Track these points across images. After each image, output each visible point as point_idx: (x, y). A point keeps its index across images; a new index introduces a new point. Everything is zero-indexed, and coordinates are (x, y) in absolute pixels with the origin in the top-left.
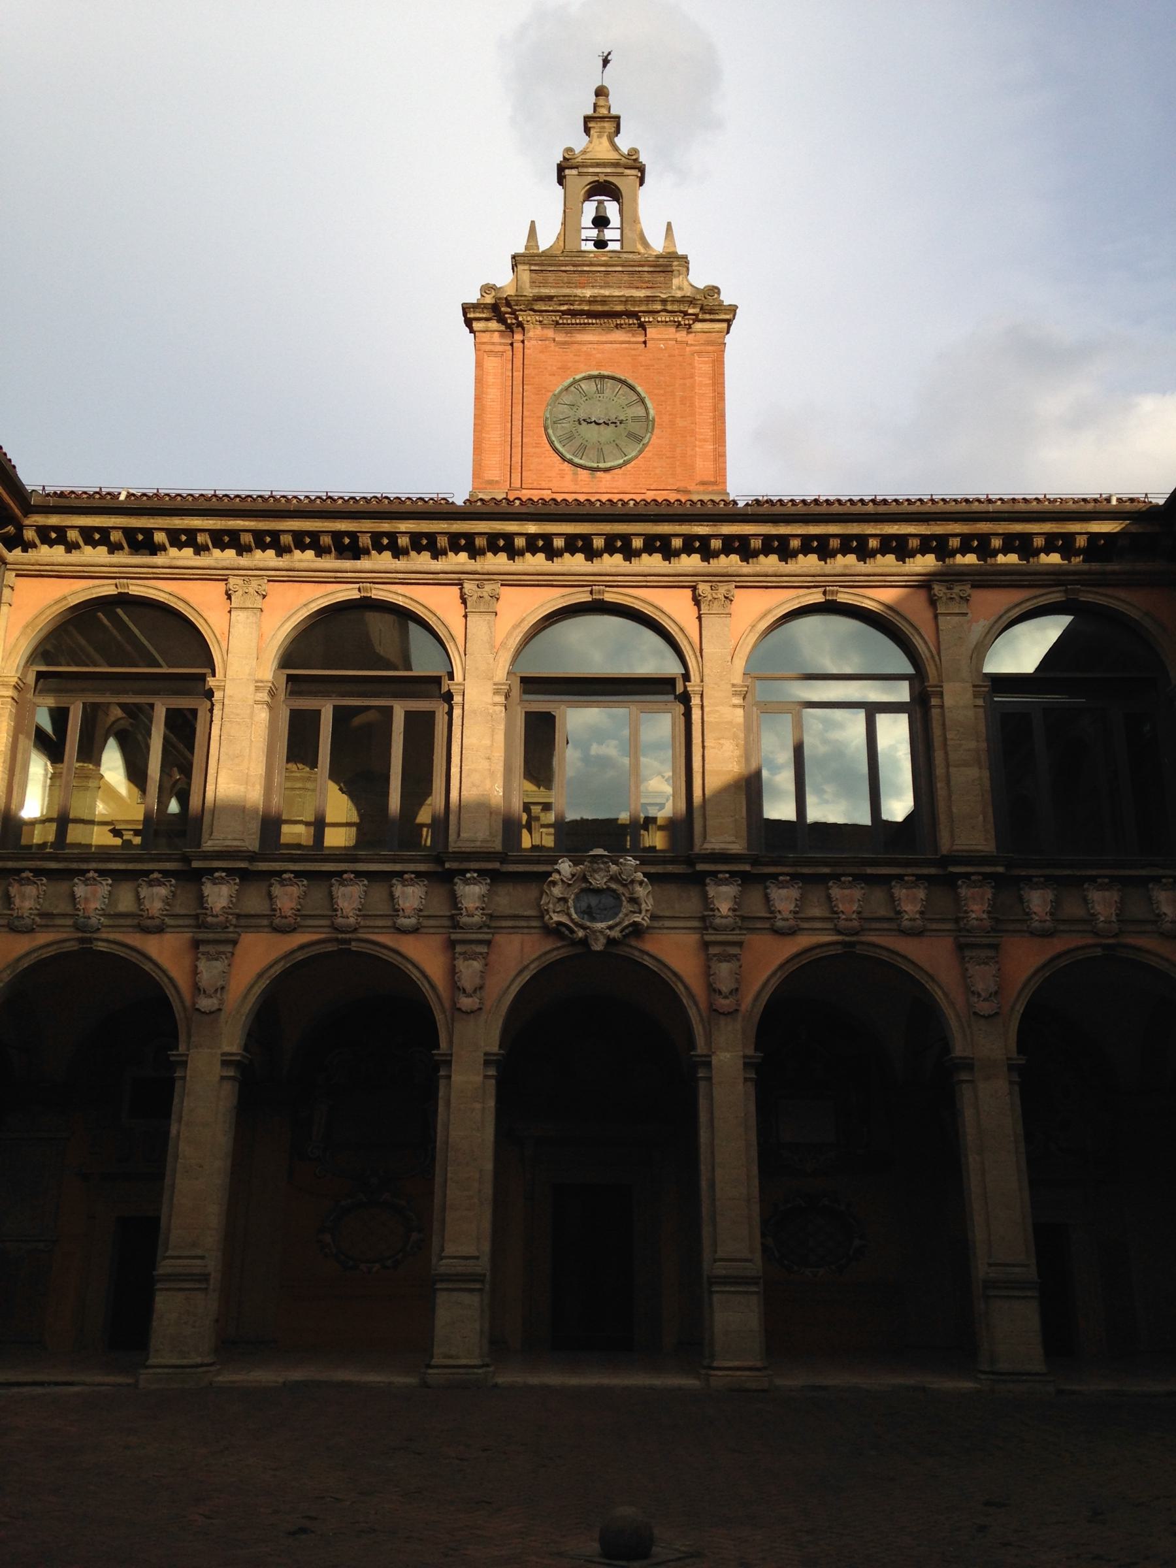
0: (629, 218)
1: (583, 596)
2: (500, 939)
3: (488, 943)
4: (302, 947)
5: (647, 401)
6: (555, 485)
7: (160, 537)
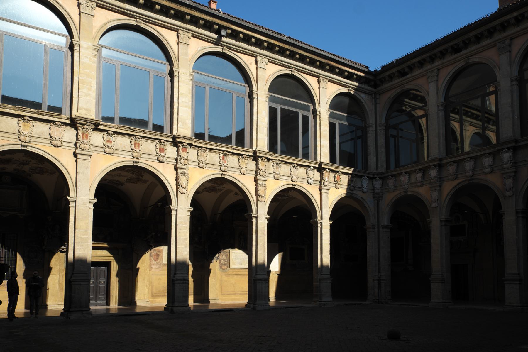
4: (458, 184)
7: (407, 70)
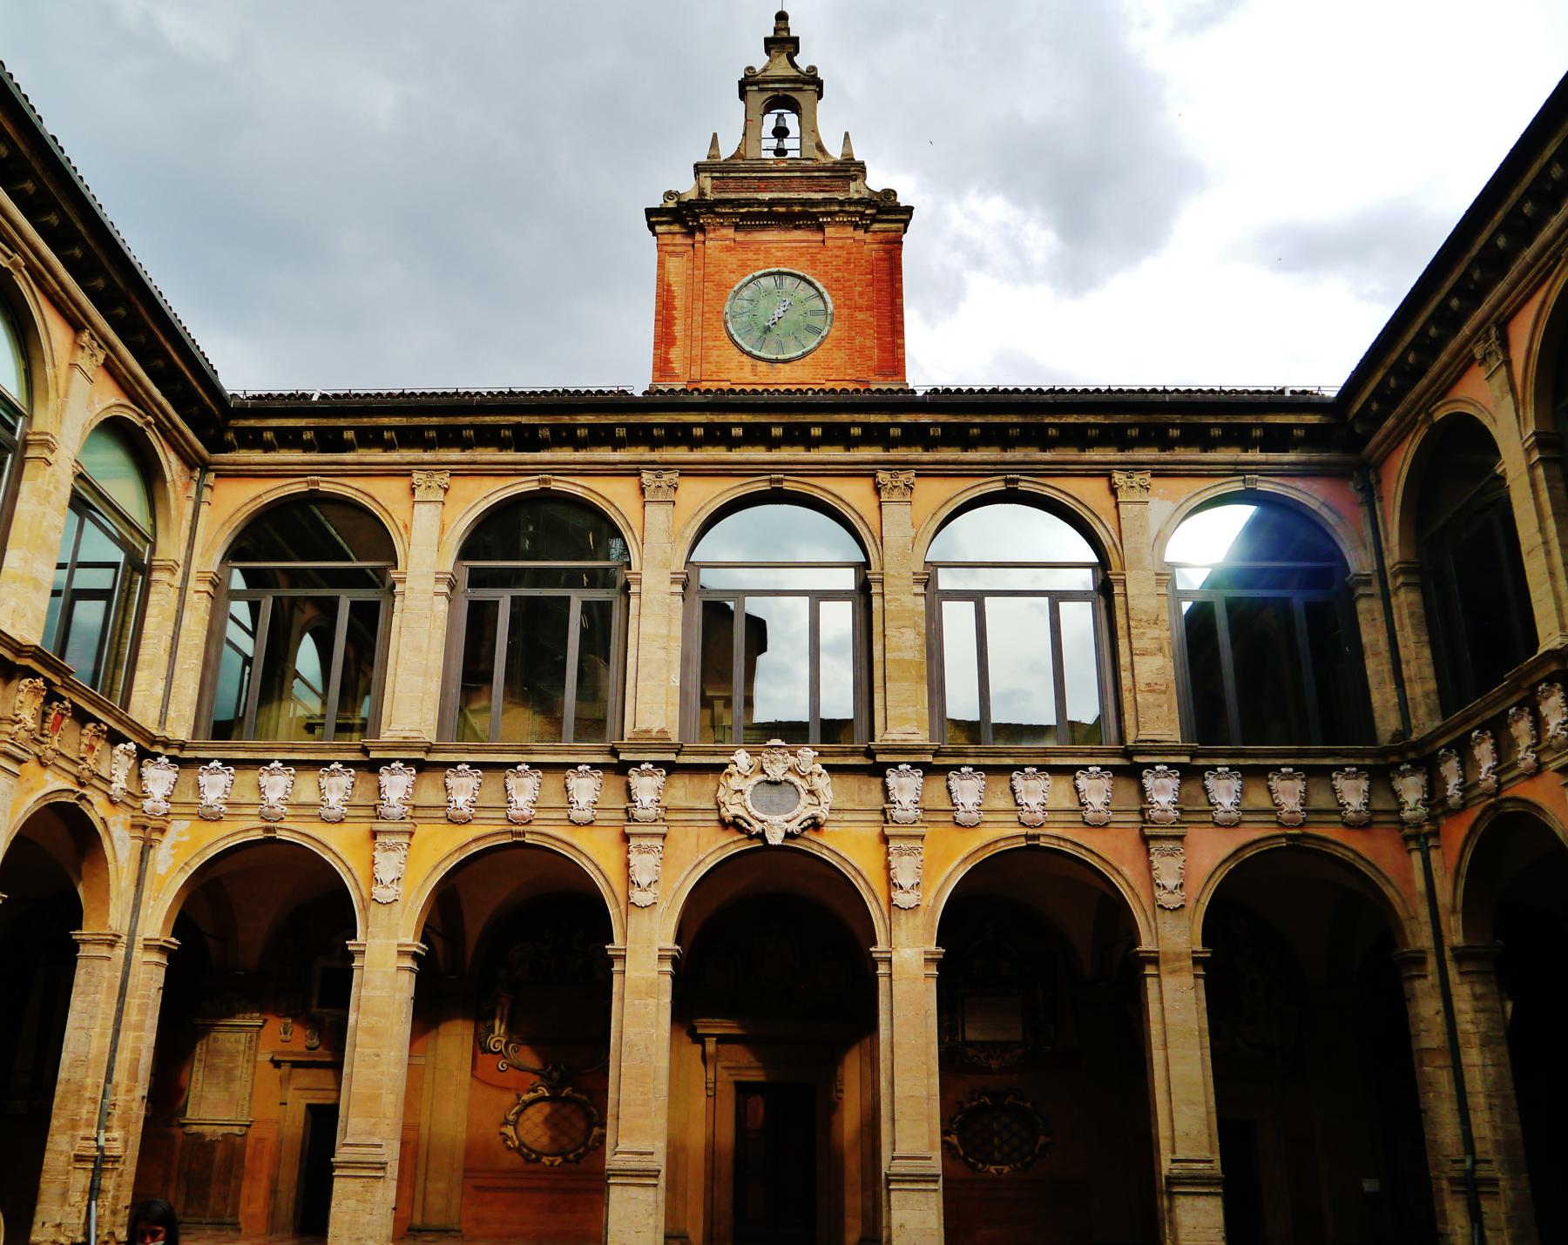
0: (809, 128)
1: (762, 486)
2: (675, 832)
3: (664, 836)
4: (476, 840)
5: (826, 295)
6: (733, 376)
